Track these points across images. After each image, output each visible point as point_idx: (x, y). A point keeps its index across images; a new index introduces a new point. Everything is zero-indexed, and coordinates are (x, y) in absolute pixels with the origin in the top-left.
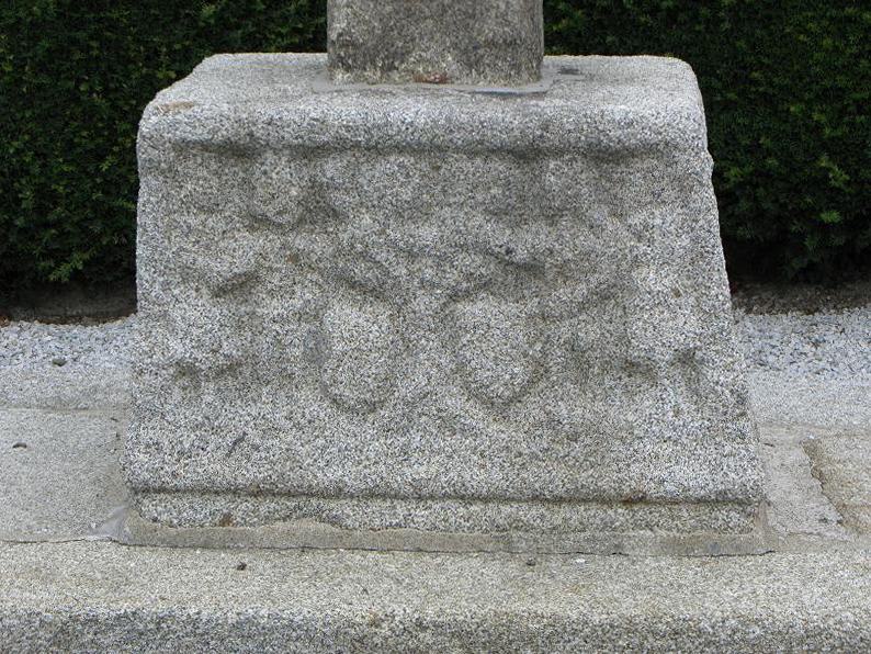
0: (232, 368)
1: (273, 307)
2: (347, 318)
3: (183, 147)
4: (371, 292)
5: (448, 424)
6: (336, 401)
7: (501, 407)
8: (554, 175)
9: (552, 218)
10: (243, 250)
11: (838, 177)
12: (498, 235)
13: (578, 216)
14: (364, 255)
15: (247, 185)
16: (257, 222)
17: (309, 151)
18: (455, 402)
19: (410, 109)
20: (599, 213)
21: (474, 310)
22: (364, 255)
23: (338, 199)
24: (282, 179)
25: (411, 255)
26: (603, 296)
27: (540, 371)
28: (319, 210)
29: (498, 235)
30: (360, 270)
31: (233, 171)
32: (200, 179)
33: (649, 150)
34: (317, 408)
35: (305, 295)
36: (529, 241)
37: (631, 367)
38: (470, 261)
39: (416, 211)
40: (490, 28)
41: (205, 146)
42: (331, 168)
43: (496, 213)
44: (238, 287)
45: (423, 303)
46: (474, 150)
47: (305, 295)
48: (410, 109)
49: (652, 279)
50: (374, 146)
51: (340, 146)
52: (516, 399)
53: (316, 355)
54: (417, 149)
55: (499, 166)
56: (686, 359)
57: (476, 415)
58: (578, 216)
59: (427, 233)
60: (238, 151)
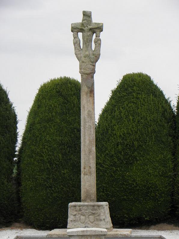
0: (74, 221)
1: (77, 216)
2: (82, 217)
3: (71, 206)
4: (84, 215)
5: (89, 224)
6: (82, 223)
7: (92, 223)
8: (95, 207)
9: (95, 210)
10: (75, 213)
11: (127, 216)
12: (92, 211)
13: (97, 210)
14: (83, 213)
15: (76, 209)
16: (76, 211)
17: (80, 206)
18: (89, 222)
19: (86, 203)
20: (98, 210)
21: (90, 216)
22: (83, 213)
23: (81, 209)
24: (78, 208)
25: (86, 213)
26: (99, 215)
27: (95, 220)
28: (80, 210)
29: (92, 211)
30: (83, 214)
31: (75, 208)
32: (73, 208)
33: (101, 206)
34: (80, 223)
35: (79, 216)
36: (94, 212)
37: (100, 220)
38: (90, 213)
39: (86, 210)
40: (92, 199)
41: (73, 206)
42: (81, 207)
43: (92, 210)
44: (75, 215)
45: (87, 216)
46: (90, 206)
47: (79, 216)
48: (86, 203)
49: (102, 214)
50: (84, 206)
51: (82, 206)
52: (93, 222)
53: (80, 219)
54: (87, 206)
55: (92, 207)
56: (104, 219)
57: (90, 223)
58: (97, 210)
59: (87, 211)
60: (75, 206)
